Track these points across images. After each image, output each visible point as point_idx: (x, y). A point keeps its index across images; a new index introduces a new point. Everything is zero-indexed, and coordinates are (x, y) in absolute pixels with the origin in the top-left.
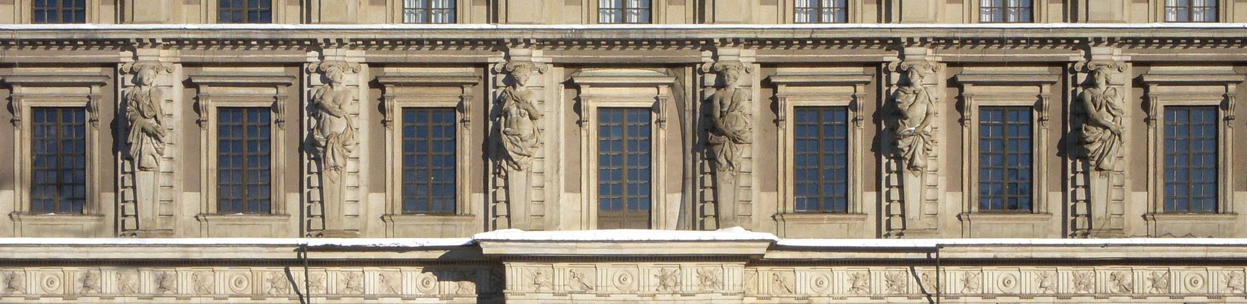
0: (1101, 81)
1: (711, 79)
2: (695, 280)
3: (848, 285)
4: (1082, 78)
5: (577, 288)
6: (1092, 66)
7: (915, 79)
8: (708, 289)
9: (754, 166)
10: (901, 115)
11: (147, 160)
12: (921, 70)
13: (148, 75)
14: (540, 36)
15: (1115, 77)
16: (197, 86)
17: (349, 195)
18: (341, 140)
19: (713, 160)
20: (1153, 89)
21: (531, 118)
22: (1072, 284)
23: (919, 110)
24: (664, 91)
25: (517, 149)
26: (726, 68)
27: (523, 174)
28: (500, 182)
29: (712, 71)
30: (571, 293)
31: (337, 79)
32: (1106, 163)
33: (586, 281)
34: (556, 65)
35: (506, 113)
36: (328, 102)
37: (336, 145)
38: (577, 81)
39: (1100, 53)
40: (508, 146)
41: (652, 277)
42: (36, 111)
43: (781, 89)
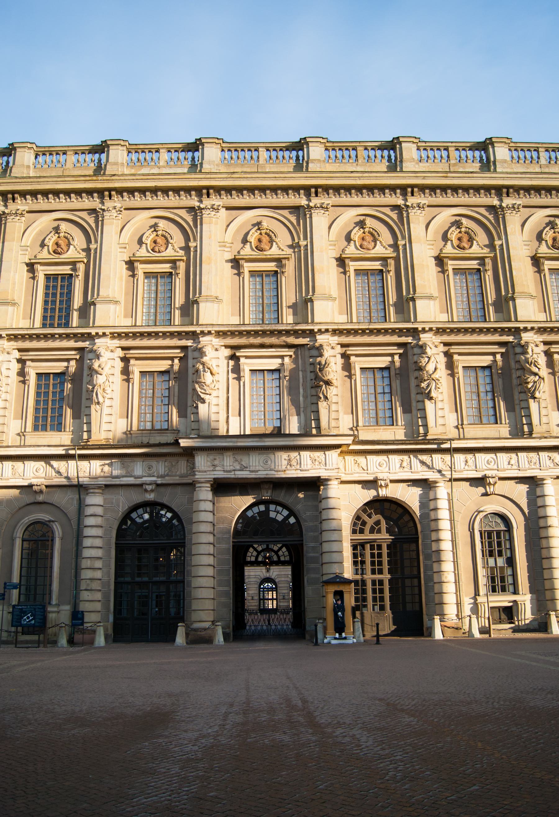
2: (309, 462)
3: (398, 465)
5: (238, 468)
7: (428, 350)
8: (317, 467)
9: (340, 400)
12: (431, 346)
14: (217, 329)
17: (105, 419)
18: (102, 388)
21: (212, 373)
22: (526, 463)
23: (430, 368)
24: (287, 360)
25: (203, 391)
26: (321, 346)
27: (206, 405)
30: (234, 470)
31: (102, 354)
33: (243, 463)
34: (226, 347)
37: (99, 390)
38: (238, 354)
39: (526, 337)
40: (199, 389)
41: (283, 460)
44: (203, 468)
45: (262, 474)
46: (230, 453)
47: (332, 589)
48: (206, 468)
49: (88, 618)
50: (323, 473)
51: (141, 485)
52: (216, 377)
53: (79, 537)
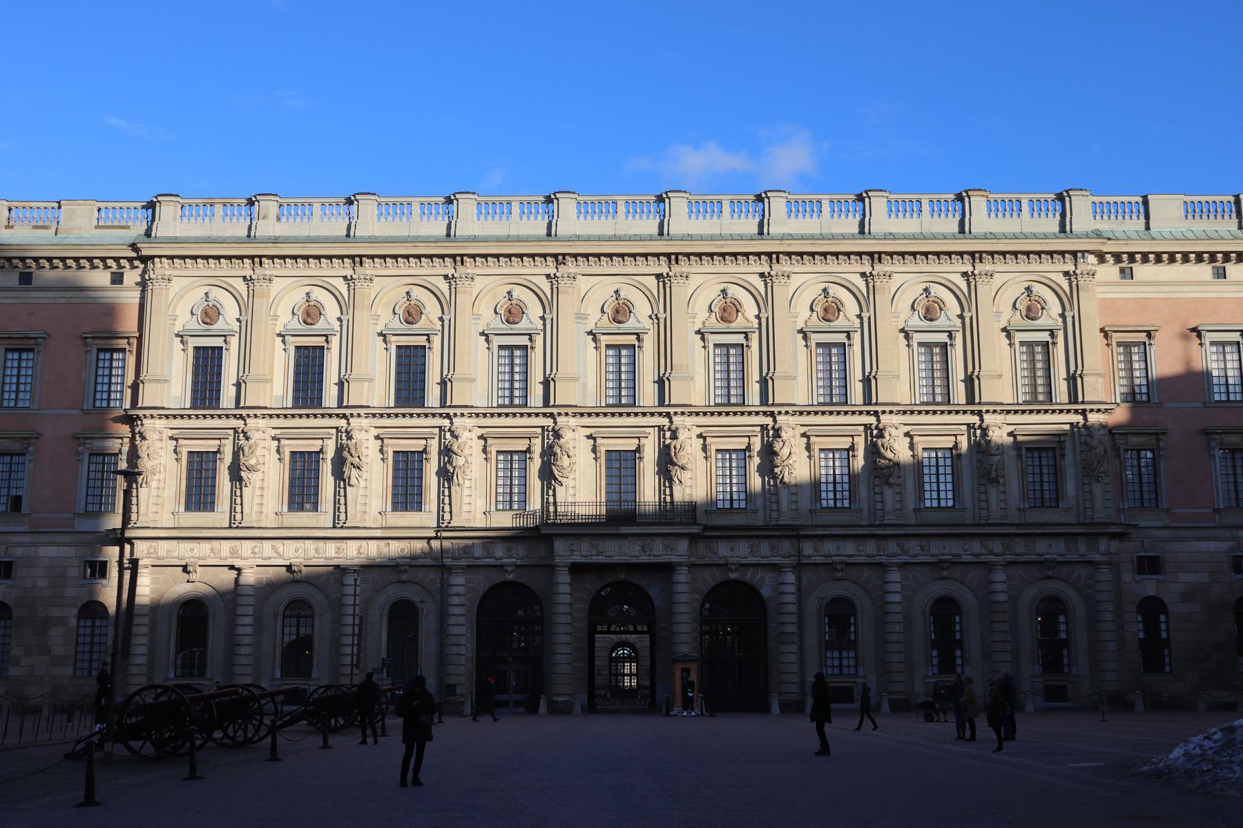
0: (887, 435)
1: (668, 434)
4: (875, 432)
6: (881, 426)
7: (783, 434)
10: (776, 454)
11: (353, 481)
13: (355, 434)
15: (894, 432)
16: (382, 439)
17: (466, 500)
19: (671, 480)
20: (916, 439)
23: (785, 452)
28: (551, 492)
29: (669, 429)
32: (891, 480)
35: (555, 454)
36: (455, 448)
40: (556, 472)
42: (293, 453)
43: (708, 440)
44: (561, 553)
45: (617, 559)
46: (587, 539)
47: (678, 667)
48: (565, 553)
49: (459, 690)
50: (674, 559)
51: (502, 566)
52: (573, 459)
53: (443, 615)
